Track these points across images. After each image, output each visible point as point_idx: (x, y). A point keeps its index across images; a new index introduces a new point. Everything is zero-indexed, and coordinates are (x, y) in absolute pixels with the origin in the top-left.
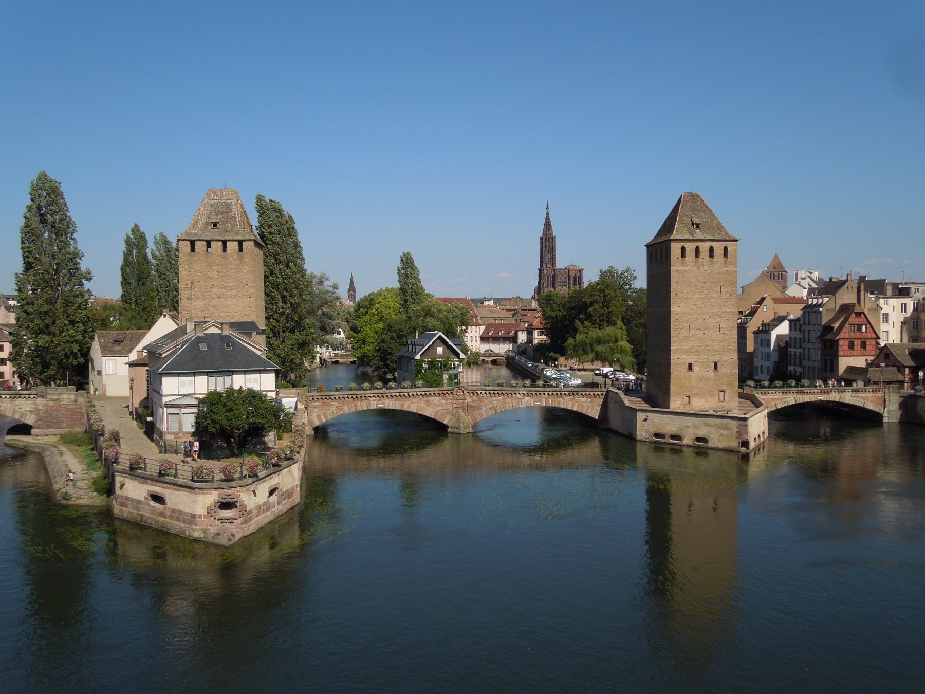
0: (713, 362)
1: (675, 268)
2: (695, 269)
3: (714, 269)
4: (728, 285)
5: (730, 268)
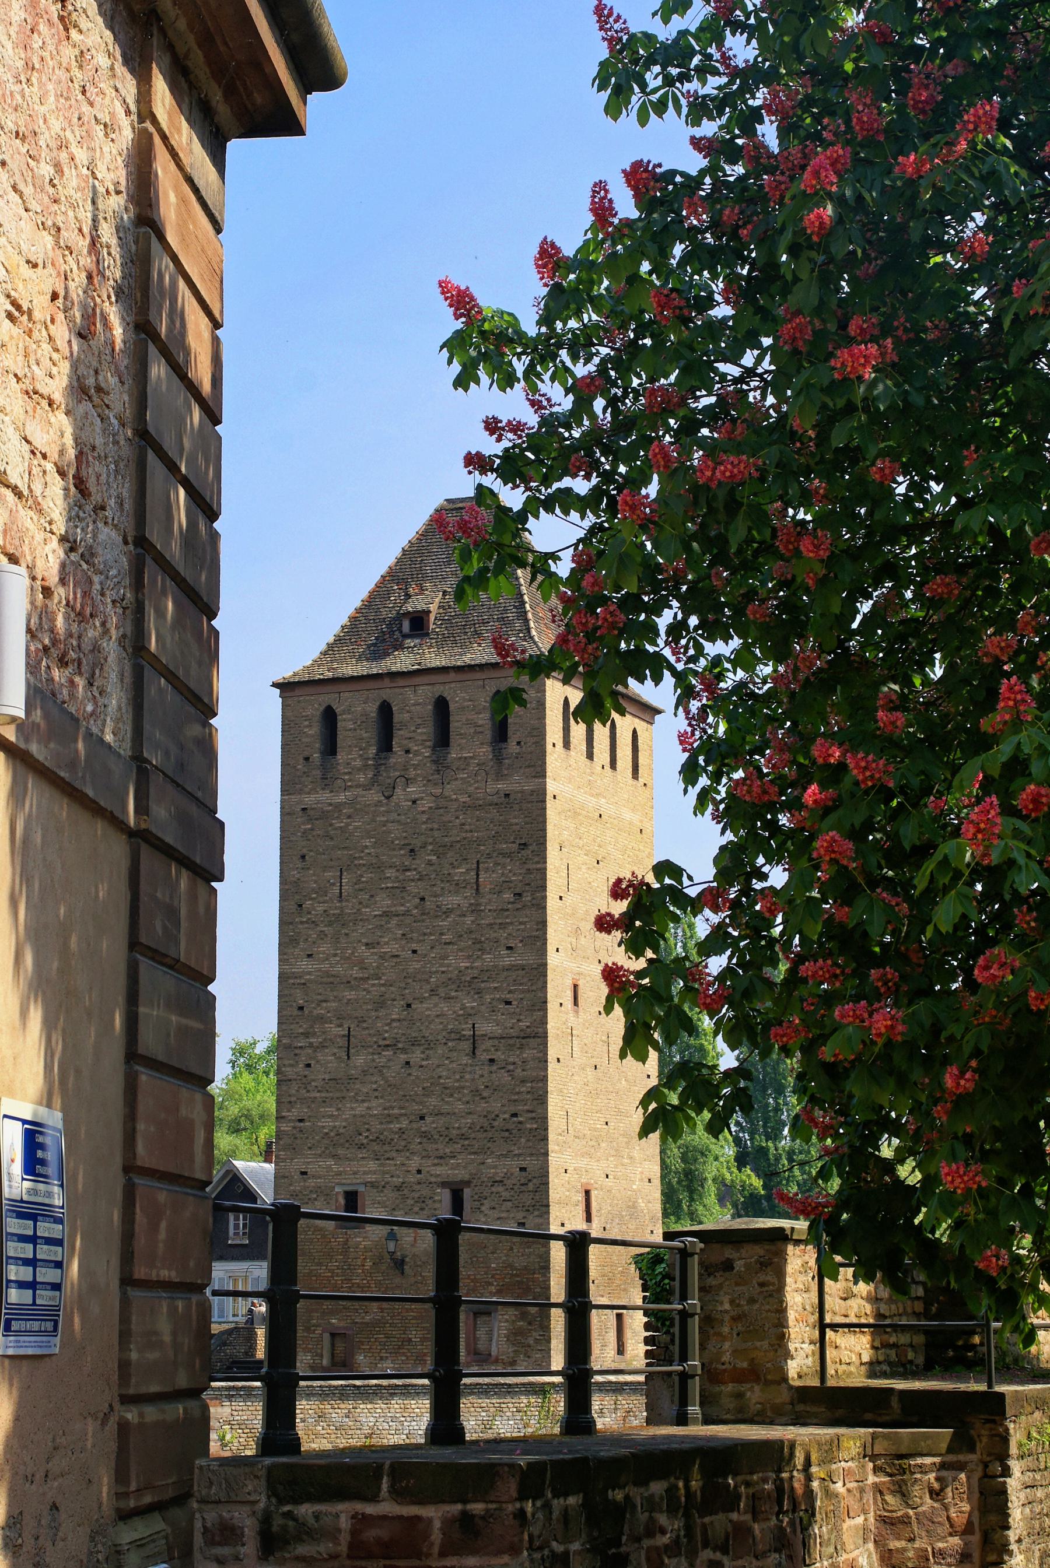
0: (444, 1185)
1: (294, 798)
2: (374, 796)
3: (449, 789)
4: (509, 855)
5: (517, 783)
